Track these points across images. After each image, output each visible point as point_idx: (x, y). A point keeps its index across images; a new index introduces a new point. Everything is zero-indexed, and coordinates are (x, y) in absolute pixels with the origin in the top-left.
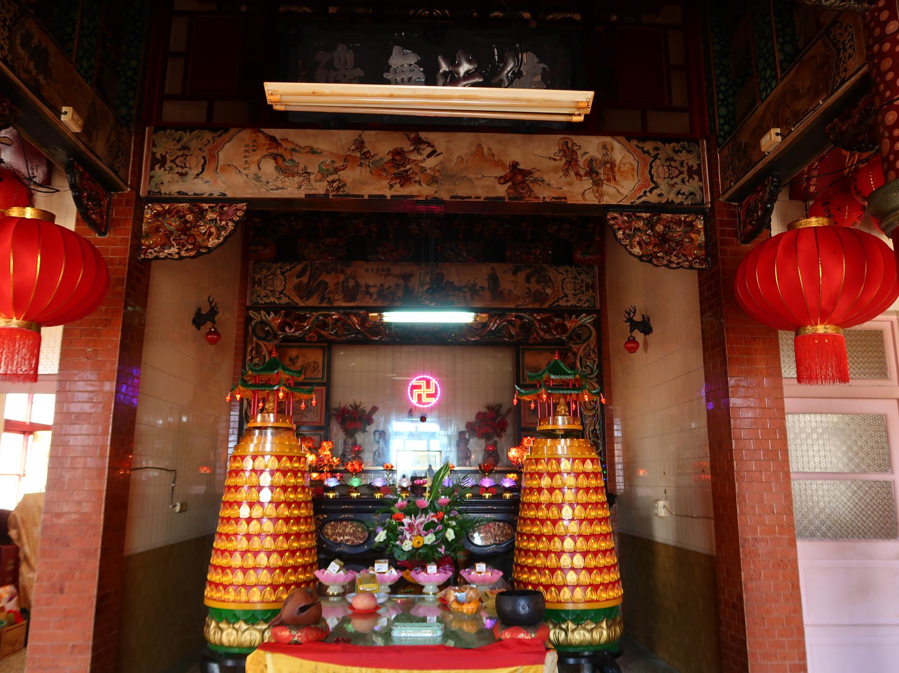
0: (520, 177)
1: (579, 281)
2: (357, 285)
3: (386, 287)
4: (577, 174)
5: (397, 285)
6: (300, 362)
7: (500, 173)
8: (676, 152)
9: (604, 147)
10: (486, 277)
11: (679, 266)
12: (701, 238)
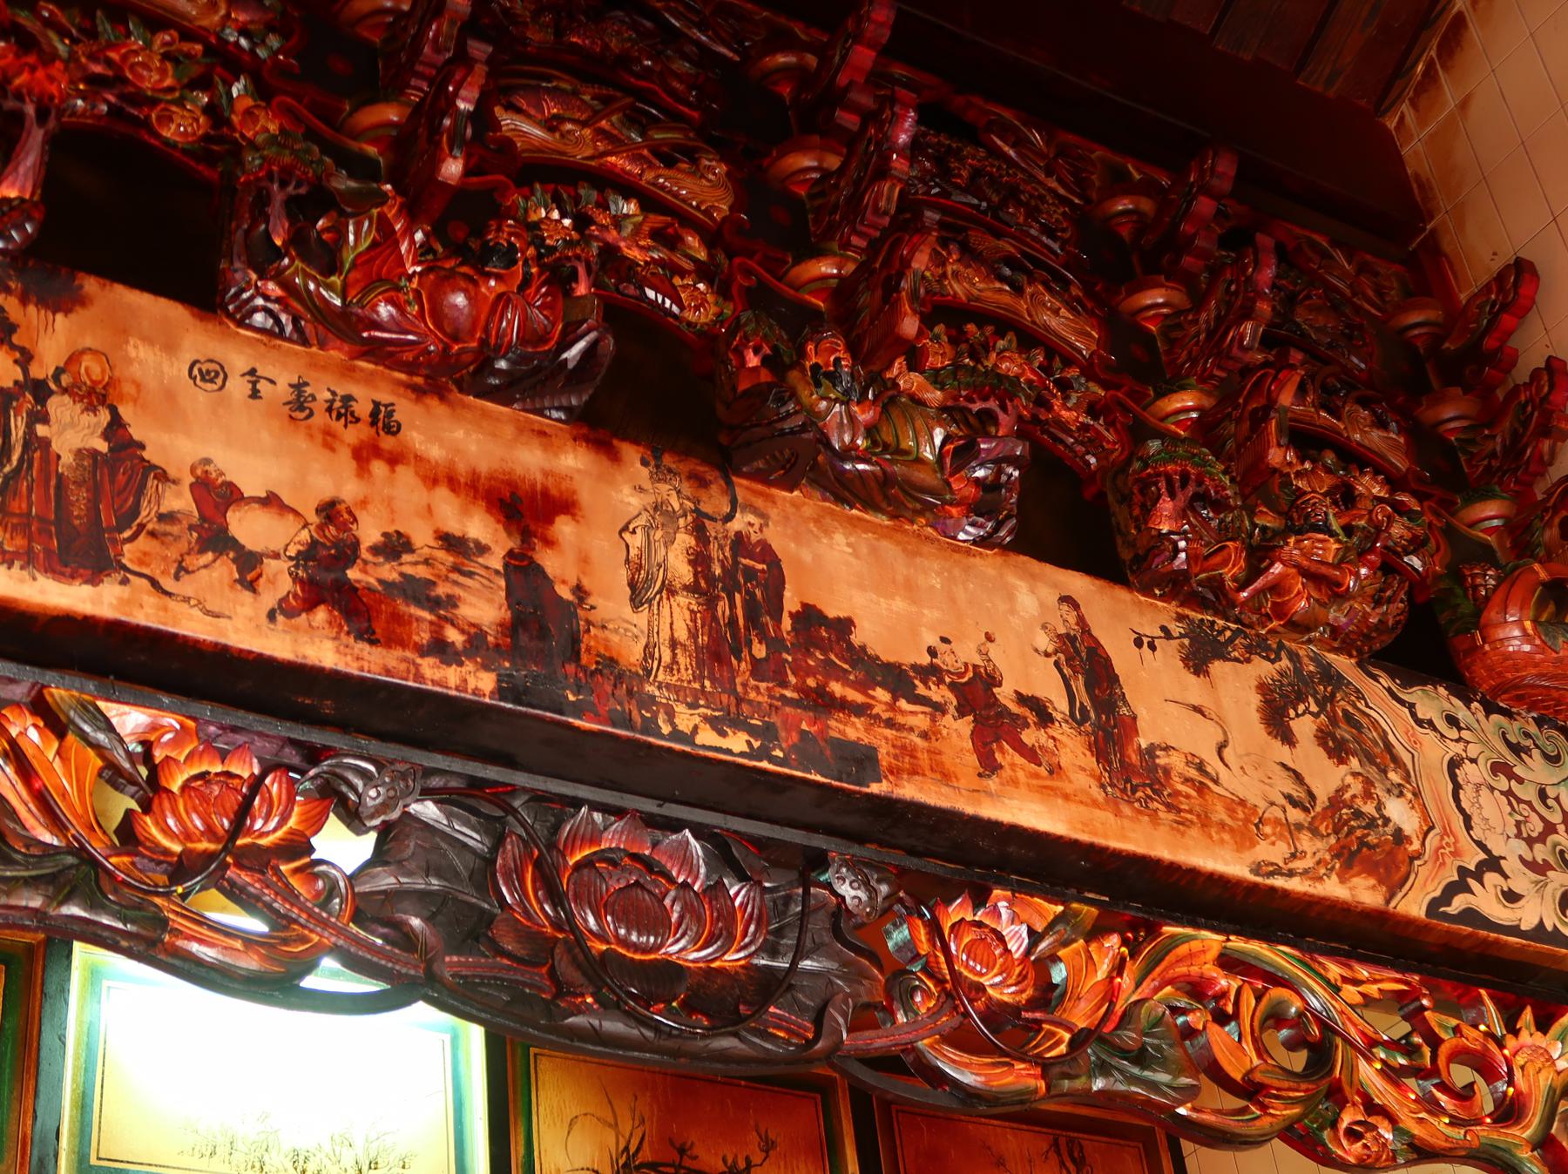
1: (1528, 793)
2: (124, 466)
3: (369, 532)
5: (451, 542)
10: (1044, 642)
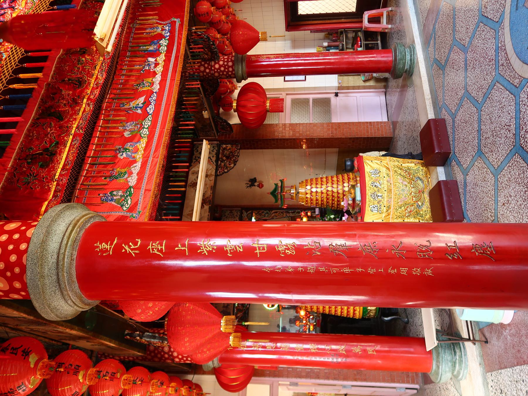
8: (197, 151)
9: (193, 173)
11: (238, 153)
12: (229, 146)
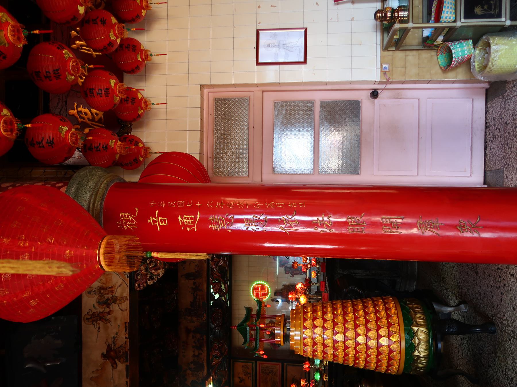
0: (112, 353)
3: (194, 344)
4: (109, 313)
6: (243, 376)
7: (109, 366)
10: (187, 281)
